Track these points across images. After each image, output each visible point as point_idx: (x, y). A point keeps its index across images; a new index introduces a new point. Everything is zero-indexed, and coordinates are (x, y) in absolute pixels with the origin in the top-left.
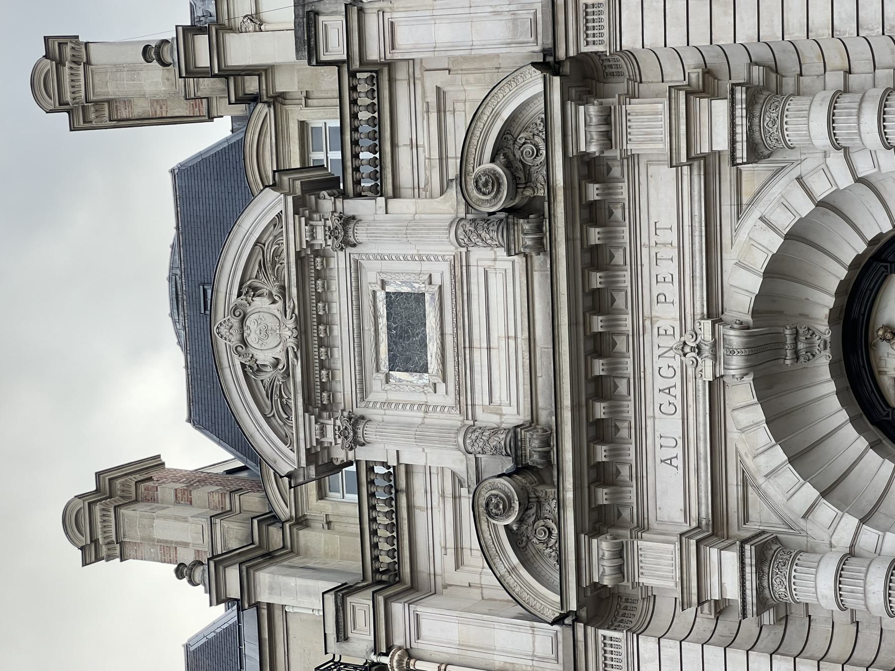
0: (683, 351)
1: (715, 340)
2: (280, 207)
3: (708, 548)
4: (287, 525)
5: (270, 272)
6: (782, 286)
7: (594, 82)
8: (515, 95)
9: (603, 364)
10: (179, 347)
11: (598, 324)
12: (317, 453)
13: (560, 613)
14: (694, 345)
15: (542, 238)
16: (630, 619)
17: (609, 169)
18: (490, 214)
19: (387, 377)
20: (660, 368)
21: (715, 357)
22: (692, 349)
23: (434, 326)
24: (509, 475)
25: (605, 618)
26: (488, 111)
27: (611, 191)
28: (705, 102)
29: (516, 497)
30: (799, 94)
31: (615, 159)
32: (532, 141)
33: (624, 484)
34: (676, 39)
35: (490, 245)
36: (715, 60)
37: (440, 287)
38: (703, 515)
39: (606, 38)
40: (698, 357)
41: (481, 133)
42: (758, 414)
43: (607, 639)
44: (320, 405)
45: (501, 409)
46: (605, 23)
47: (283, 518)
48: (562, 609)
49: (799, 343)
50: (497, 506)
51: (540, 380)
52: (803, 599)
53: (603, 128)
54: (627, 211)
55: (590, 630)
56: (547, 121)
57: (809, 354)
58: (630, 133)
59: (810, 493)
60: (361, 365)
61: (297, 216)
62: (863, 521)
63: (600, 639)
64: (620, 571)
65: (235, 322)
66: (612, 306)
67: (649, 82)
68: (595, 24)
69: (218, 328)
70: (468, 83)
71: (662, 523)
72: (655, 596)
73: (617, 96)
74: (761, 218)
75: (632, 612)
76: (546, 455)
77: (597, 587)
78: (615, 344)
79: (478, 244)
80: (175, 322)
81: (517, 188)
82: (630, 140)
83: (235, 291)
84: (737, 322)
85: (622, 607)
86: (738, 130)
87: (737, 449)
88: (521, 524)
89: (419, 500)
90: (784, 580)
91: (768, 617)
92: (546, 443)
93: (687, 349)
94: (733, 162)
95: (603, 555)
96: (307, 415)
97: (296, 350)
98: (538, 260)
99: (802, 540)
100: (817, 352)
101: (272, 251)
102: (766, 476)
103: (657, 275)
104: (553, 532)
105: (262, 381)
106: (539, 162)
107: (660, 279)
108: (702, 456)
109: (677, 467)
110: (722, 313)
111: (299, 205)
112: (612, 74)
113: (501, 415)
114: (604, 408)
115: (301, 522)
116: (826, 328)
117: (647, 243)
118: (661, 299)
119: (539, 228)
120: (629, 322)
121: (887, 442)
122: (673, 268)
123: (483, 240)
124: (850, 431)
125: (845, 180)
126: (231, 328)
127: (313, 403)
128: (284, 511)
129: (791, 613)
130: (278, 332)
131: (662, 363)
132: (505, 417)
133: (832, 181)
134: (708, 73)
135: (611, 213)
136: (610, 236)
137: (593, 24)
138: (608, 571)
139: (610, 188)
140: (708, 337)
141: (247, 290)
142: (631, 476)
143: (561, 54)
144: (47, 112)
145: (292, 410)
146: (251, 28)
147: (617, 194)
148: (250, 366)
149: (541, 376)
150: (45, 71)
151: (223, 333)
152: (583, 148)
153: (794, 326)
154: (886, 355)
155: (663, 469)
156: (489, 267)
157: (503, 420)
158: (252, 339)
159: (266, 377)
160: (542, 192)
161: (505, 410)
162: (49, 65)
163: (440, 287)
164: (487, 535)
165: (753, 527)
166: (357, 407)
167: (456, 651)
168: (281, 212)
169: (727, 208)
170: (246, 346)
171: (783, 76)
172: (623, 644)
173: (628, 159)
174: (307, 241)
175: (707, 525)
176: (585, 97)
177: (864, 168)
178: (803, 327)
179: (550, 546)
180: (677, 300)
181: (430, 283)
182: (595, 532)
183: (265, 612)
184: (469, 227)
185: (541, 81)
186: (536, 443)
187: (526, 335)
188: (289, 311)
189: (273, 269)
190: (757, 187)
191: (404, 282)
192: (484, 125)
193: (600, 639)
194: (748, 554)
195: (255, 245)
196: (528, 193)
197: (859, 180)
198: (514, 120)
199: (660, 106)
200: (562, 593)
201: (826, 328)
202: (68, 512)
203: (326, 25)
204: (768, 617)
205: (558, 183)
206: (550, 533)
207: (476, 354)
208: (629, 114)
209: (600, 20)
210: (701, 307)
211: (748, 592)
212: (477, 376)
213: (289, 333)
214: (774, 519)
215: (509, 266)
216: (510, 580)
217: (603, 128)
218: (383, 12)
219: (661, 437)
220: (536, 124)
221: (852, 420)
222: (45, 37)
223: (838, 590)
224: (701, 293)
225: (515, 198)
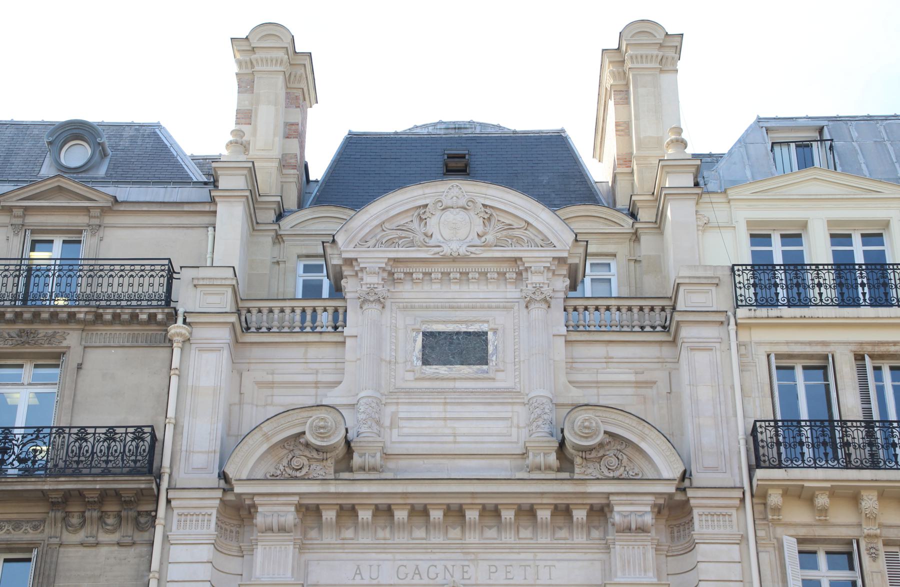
2: (559, 246)
4: (276, 227)
5: (505, 233)
7: (666, 517)
9: (439, 518)
10: (412, 126)
12: (351, 265)
13: (231, 479)
19: (418, 331)
23: (461, 372)
27: (580, 529)
31: (606, 532)
37: (494, 379)
41: (628, 424)
44: (393, 271)
45: (395, 428)
47: (282, 223)
48: (236, 480)
60: (427, 307)
61: (551, 259)
63: (209, 511)
65: (462, 202)
66: (486, 526)
67: (667, 563)
69: (457, 186)
72: (243, 556)
73: (658, 538)
75: (228, 537)
79: (533, 415)
80: (435, 125)
81: (582, 452)
83: (487, 203)
85: (232, 528)
89: (313, 352)
92: (373, 469)
96: (386, 260)
97: (442, 254)
101: (522, 237)
103: (511, 566)
104: (298, 472)
105: (412, 221)
107: (509, 569)
109: (354, 579)
111: (561, 260)
112: (672, 532)
115: (278, 239)
117: (538, 558)
119: (549, 468)
120: (472, 541)
126: (457, 197)
127: (394, 265)
128: (287, 223)
130: (454, 239)
132: (389, 430)
139: (582, 528)
141: (489, 213)
144: (620, 33)
145: (388, 247)
146: (700, 223)
148: (425, 212)
149: (424, 463)
150: (656, 34)
151: (452, 190)
156: (512, 422)
157: (386, 429)
158: (449, 215)
159: (415, 225)
160: (578, 472)
162: (660, 37)
163: (494, 379)
166: (392, 302)
167: (190, 384)
168: (555, 247)
170: (443, 210)
172: (205, 531)
173: (606, 544)
174: (531, 267)
176: (656, 510)
179: (286, 469)
181: (497, 371)
182: (299, 507)
183: (207, 208)
185: (671, 476)
188: (473, 249)
189: (506, 237)
191: (496, 348)
192: (634, 427)
193: (209, 511)
195: (526, 222)
196: (578, 460)
202: (279, 28)
203: (708, 292)
205: (589, 487)
206: (297, 470)
208: (644, 548)
213: (455, 249)
215: (514, 438)
218: (720, 342)
219: (379, 566)
220: (633, 469)
222: (682, 34)
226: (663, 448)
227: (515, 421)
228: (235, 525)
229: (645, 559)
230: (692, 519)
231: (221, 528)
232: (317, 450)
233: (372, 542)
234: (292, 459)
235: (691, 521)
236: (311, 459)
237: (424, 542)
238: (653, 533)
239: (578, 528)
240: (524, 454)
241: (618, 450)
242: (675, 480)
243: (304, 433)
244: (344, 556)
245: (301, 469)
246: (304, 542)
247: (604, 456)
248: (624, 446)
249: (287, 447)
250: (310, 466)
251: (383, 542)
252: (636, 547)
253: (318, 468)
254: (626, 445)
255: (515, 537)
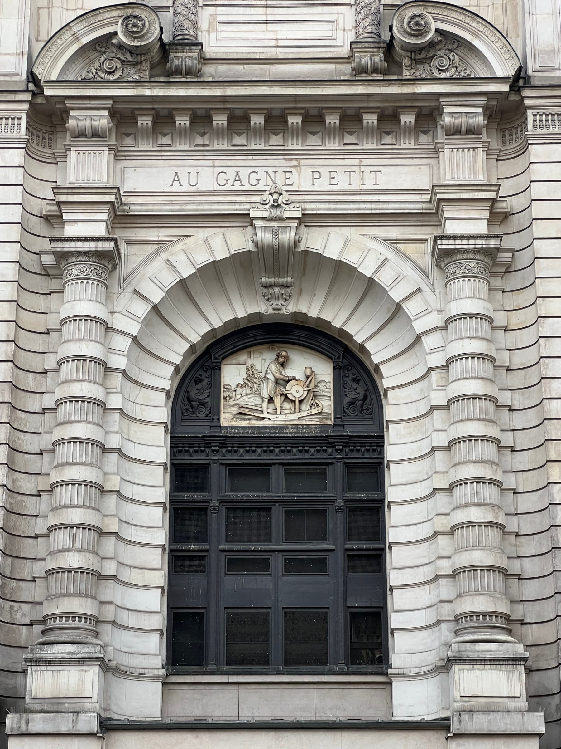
0: (275, 192)
1: (285, 220)
3: (108, 211)
6: (326, 277)
7: (498, 120)
8: (493, 51)
9: (260, 123)
11: (295, 120)
13: (41, 80)
14: (280, 202)
15: (366, 73)
16: (35, 141)
17: (425, 133)
18: (391, 28)
20: (257, 173)
21: (270, 219)
22: (276, 201)
24: (161, 39)
25: (34, 119)
26: (480, 27)
27: (407, 134)
28: (487, 214)
29: (143, 43)
30: (490, 290)
31: (435, 136)
32: (451, 66)
33: (155, 140)
34: (538, 191)
35: (358, 25)
36: (516, 222)
38: (132, 207)
39: (539, 131)
40: (269, 205)
42: (221, 254)
43: (19, 121)
45: (214, 32)
46: (551, 131)
48: (45, 82)
49: (279, 288)
50: (135, 26)
51: (240, 67)
52: (69, 289)
53: (464, 128)
54: (390, 147)
55: (26, 106)
56: (467, 79)
57: (269, 296)
58: (458, 151)
59: (157, 296)
62: (135, 339)
63: (19, 115)
64: (81, 134)
68: (550, 122)
70: (495, 9)
71: (123, 172)
72: (56, 164)
73: (489, 140)
74: (386, 259)
76: (178, 71)
77: (65, 114)
78: (276, 134)
79: (360, 15)
81: (411, 52)
82: (452, 151)
84: (300, 239)
85: (44, 135)
86: (465, 242)
87: (190, 236)
88: (117, 47)
90: (85, 274)
91: (48, 260)
92: (189, 72)
93: (276, 196)
94: (438, 237)
95: (94, 120)
98: (346, 69)
99: (115, 289)
100: (271, 303)
102: (168, 260)
103: (336, 171)
104: (111, 76)
106: (433, 72)
107: (333, 175)
108: (183, 207)
109: (172, 185)
110: (306, 226)
112: (504, 136)
113: (209, 31)
114: (222, 124)
116: (291, 310)
117: (363, 164)
118: (316, 175)
119: (375, 70)
120: (295, 147)
121: (193, 357)
122: (343, 186)
123: (363, 20)
124: (205, 329)
125: (419, 326)
129: (51, 279)
131: (261, 174)
132: (207, 34)
133: (419, 316)
134: (506, 216)
135: (388, 133)
136: (369, 132)
137: (538, 120)
138: (81, 124)
139: (410, 133)
140: (287, 214)
142: (161, 146)
143: (527, 93)
147: (405, 139)
149: (244, 68)
152: (446, 110)
153: (293, 285)
154: (264, 358)
155: (169, 174)
156: (337, 24)
157: (204, 33)
160: (407, 73)
161: (213, 35)
164: (107, 15)
165: (124, 248)
169: (393, 231)
171: (502, 277)
172: (15, 135)
173: (434, 149)
175: (124, 211)
176: (488, 112)
177: (429, 342)
178: (292, 292)
179: (98, 72)
180: (316, 188)
182: (113, 114)
184: (374, 7)
185: (506, 75)
186: (189, 62)
187: (281, 56)
190: (411, 255)
192: (468, 24)
193: (19, 115)
194: (106, 244)
196: (406, 61)
197: (418, 338)
198: (469, 50)
199: (481, 177)
200: (58, 82)
201: (291, 310)
204: (48, 260)
205: (419, 88)
206: (110, 73)
207: (261, 10)
208: (474, 150)
209: (554, 127)
210: (312, 208)
211: (73, 244)
212: (241, 10)
214: (131, 267)
216: (67, 36)
217: (464, 128)
220: (465, 70)
221: (213, 331)
223: (80, 318)
224: (323, 208)
225: (402, 49)
226: (498, 45)
227: (341, 22)
228: (47, 131)
229: (475, 162)
230: (525, 122)
231: (33, 134)
232: (131, 53)
233: (190, 149)
234: (104, 61)
235: (524, 122)
236: (124, 61)
237: (245, 148)
238: (484, 137)
239: (405, 133)
240: (349, 58)
241: (449, 50)
242: (510, 78)
243: (116, 33)
244: (161, 163)
245: (114, 72)
246: (120, 149)
247: (435, 55)
248: (455, 46)
249: (99, 49)
250: (123, 69)
251: (202, 148)
252: (466, 150)
253: (132, 71)
254: (458, 44)
255: (339, 142)
